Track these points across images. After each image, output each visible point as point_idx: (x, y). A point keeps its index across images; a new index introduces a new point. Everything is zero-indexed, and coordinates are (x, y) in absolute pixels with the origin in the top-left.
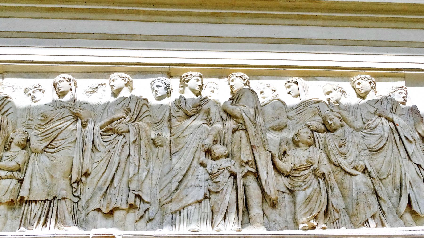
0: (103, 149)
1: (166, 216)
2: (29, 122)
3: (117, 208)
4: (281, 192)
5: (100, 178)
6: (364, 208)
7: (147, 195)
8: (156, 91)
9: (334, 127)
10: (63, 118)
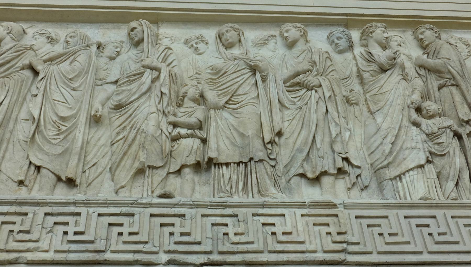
0: (293, 106)
1: (385, 183)
2: (197, 76)
3: (325, 173)
5: (297, 139)
7: (356, 159)
8: (337, 44)
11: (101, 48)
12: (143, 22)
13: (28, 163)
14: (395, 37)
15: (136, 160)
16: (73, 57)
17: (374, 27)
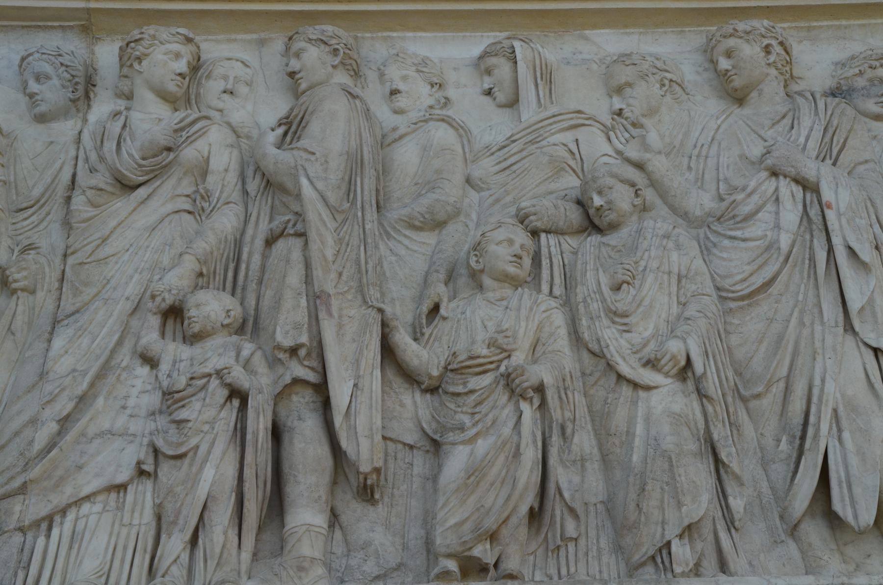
4: (405, 444)
6: (662, 501)
9: (612, 217)
14: (226, 63)
17: (145, 43)
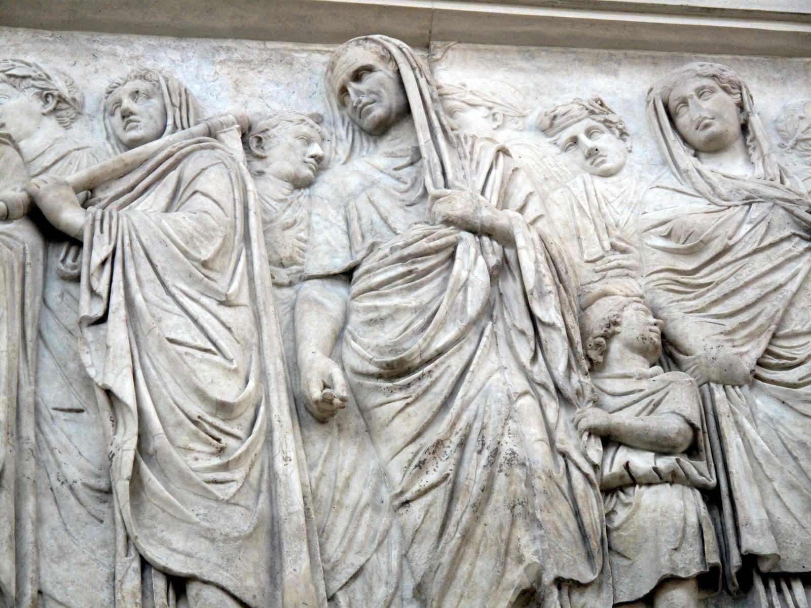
10: (772, 245)
11: (253, 144)
12: (393, 44)
13: (136, 564)
15: (509, 560)
16: (172, 177)
